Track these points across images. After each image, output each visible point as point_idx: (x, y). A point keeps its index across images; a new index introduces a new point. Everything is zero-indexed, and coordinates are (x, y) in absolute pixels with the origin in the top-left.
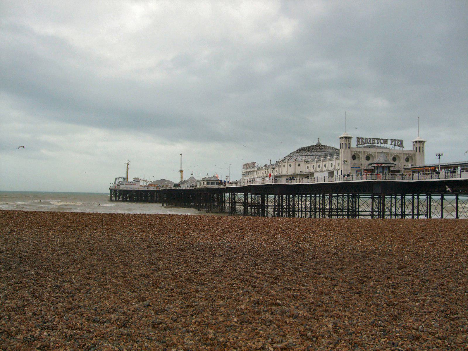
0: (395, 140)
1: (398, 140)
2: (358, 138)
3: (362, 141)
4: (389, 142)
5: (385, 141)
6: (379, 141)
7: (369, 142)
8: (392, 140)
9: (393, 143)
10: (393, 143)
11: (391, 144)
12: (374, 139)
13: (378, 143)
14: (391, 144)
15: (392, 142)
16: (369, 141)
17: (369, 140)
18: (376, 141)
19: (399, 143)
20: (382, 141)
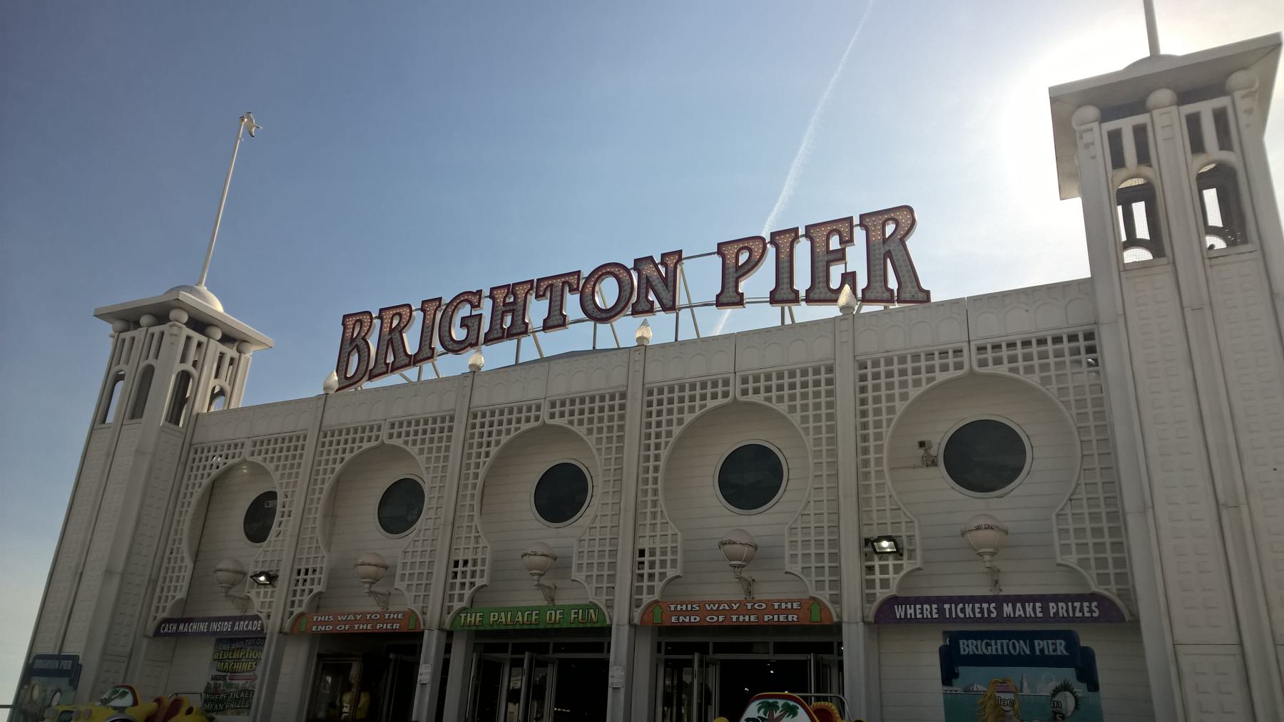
0: (784, 239)
1: (842, 227)
2: (355, 323)
3: (392, 339)
4: (701, 279)
5: (653, 284)
6: (572, 305)
7: (458, 333)
8: (744, 243)
9: (759, 282)
10: (759, 282)
11: (729, 297)
12: (511, 289)
13: (556, 321)
14: (729, 297)
15: (733, 274)
16: (464, 323)
17: (465, 311)
18: (537, 311)
19: (840, 256)
20: (607, 293)
